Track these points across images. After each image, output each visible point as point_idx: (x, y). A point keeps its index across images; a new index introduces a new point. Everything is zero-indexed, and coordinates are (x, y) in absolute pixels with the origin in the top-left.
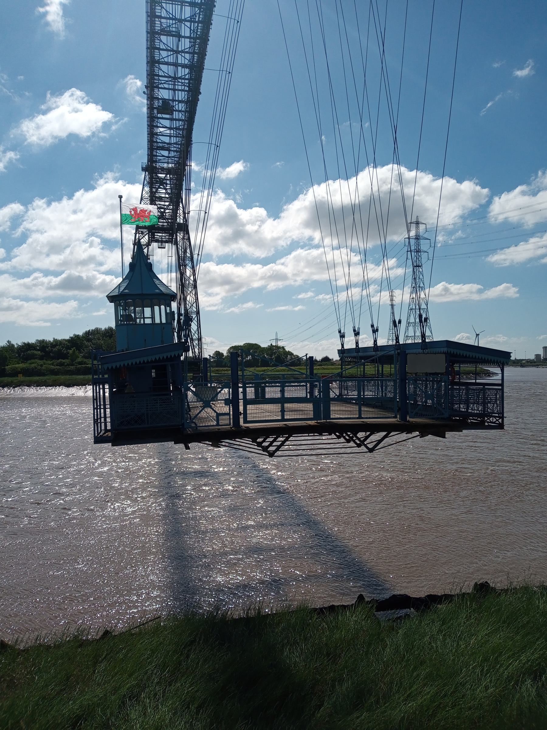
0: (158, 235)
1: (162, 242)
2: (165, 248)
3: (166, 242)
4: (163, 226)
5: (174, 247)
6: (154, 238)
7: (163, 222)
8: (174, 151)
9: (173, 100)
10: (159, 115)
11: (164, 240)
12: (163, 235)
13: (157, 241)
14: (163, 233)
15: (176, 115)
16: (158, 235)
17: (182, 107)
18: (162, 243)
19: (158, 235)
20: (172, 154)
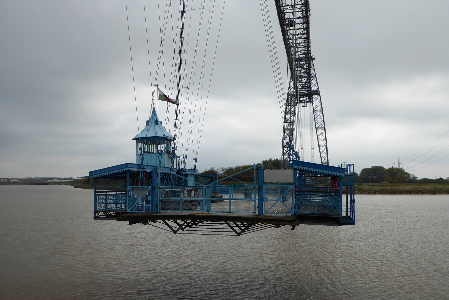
0: (302, 99)
1: (304, 103)
2: (306, 106)
3: (307, 102)
4: (303, 93)
5: (312, 104)
6: (299, 100)
7: (303, 91)
8: (300, 47)
9: (294, 18)
10: (288, 28)
11: (306, 101)
12: (304, 98)
13: (301, 102)
14: (304, 97)
15: (297, 26)
16: (301, 99)
17: (300, 21)
18: (304, 103)
19: (301, 99)
20: (300, 49)
